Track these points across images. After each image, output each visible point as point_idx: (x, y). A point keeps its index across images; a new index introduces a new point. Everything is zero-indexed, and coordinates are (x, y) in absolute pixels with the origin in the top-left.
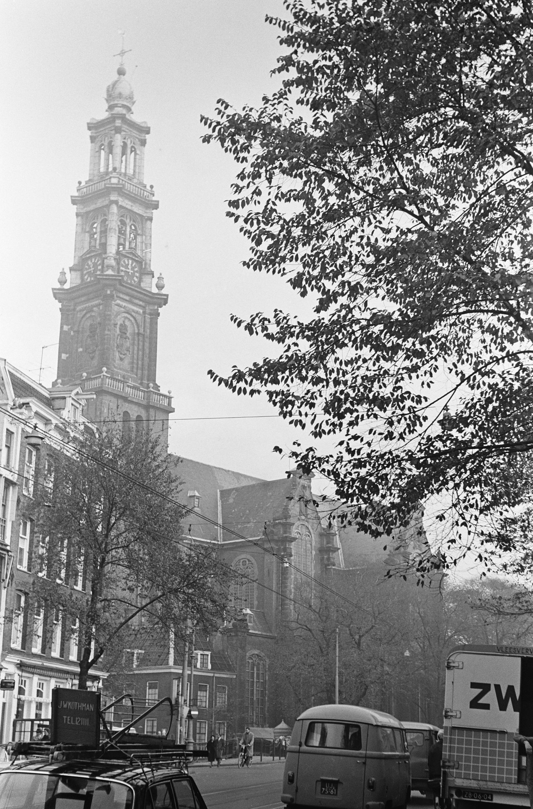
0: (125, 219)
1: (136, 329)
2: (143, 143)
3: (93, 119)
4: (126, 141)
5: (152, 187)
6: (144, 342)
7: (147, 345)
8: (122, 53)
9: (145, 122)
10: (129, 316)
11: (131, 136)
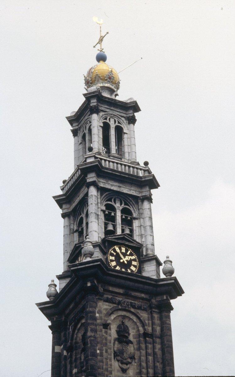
0: (113, 203)
1: (141, 329)
2: (132, 120)
3: (74, 112)
4: (108, 121)
5: (146, 164)
6: (154, 342)
7: (158, 346)
8: (101, 40)
9: (131, 99)
10: (128, 314)
11: (113, 116)
